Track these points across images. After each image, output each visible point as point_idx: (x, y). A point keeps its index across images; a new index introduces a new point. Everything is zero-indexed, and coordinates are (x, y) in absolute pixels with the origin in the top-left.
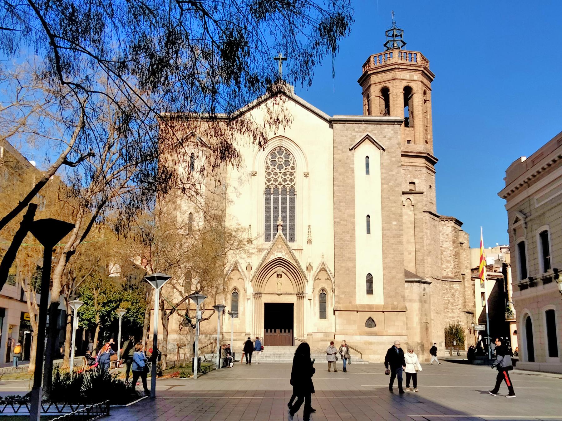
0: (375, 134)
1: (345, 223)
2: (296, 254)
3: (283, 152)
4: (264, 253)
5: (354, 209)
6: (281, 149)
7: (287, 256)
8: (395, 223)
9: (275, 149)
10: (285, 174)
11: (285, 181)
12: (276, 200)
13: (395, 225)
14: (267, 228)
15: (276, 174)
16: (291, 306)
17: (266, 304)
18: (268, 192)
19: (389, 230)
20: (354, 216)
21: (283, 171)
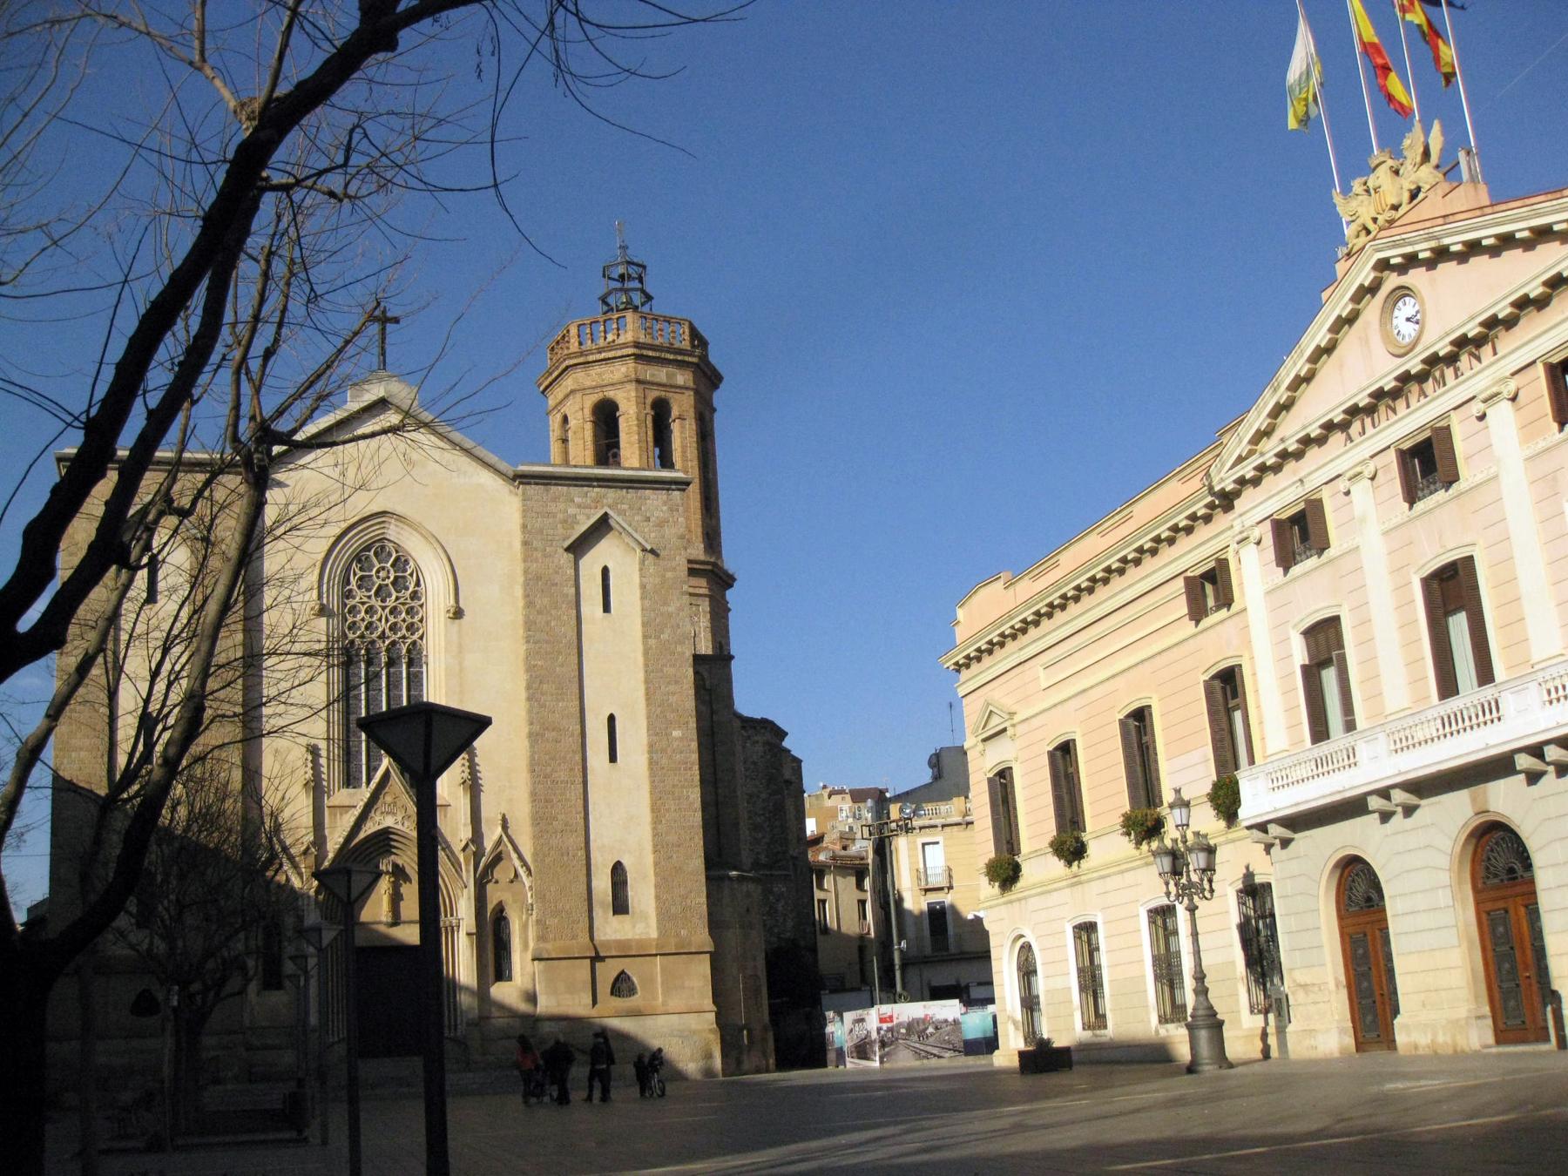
3: (390, 555)
8: (676, 733)
13: (681, 739)
19: (663, 751)
21: (390, 602)
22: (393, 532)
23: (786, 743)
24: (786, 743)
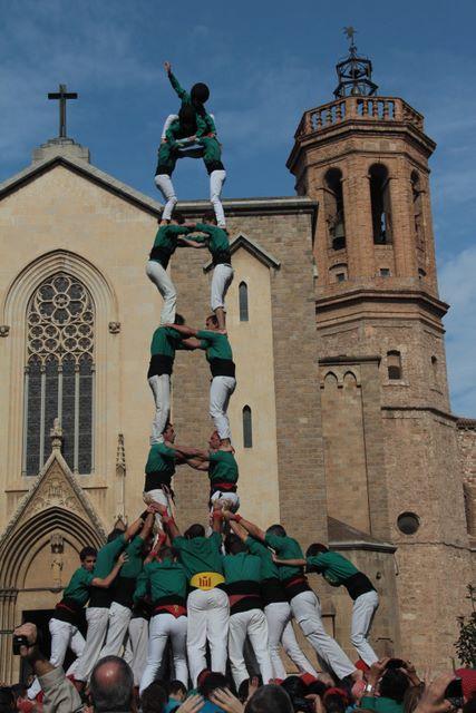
1: (196, 425)
2: (92, 500)
4: (22, 500)
7: (70, 504)
8: (304, 420)
9: (49, 280)
10: (70, 330)
11: (70, 343)
12: (52, 385)
13: (305, 425)
14: (32, 445)
15: (51, 330)
18: (33, 370)
19: (291, 436)
21: (67, 323)
22: (70, 266)
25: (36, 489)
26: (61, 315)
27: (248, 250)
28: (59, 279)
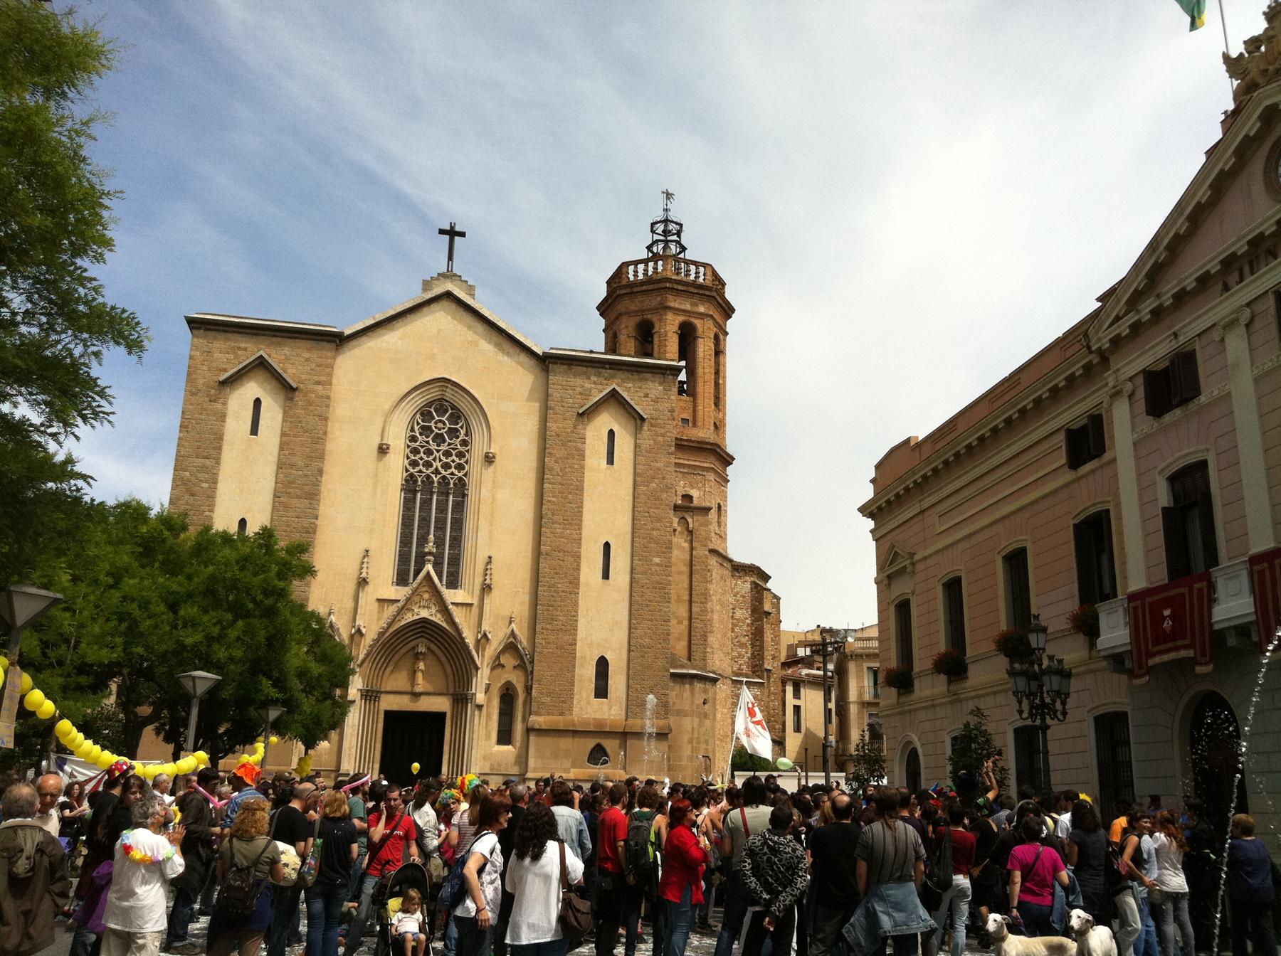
0: (628, 390)
1: (561, 554)
4: (393, 609)
5: (580, 529)
6: (442, 406)
9: (429, 405)
10: (447, 454)
11: (446, 466)
12: (426, 504)
14: (403, 558)
16: (441, 716)
17: (389, 715)
18: (410, 486)
19: (644, 573)
20: (578, 542)
21: (444, 447)
22: (449, 394)
23: (769, 585)
24: (769, 585)
25: (408, 600)
26: (439, 439)
27: (620, 403)
28: (441, 405)
